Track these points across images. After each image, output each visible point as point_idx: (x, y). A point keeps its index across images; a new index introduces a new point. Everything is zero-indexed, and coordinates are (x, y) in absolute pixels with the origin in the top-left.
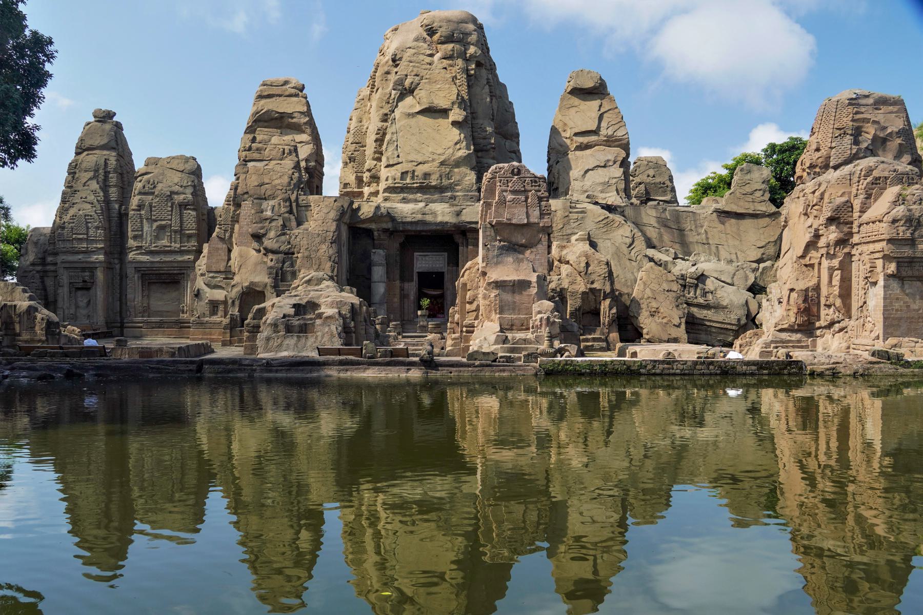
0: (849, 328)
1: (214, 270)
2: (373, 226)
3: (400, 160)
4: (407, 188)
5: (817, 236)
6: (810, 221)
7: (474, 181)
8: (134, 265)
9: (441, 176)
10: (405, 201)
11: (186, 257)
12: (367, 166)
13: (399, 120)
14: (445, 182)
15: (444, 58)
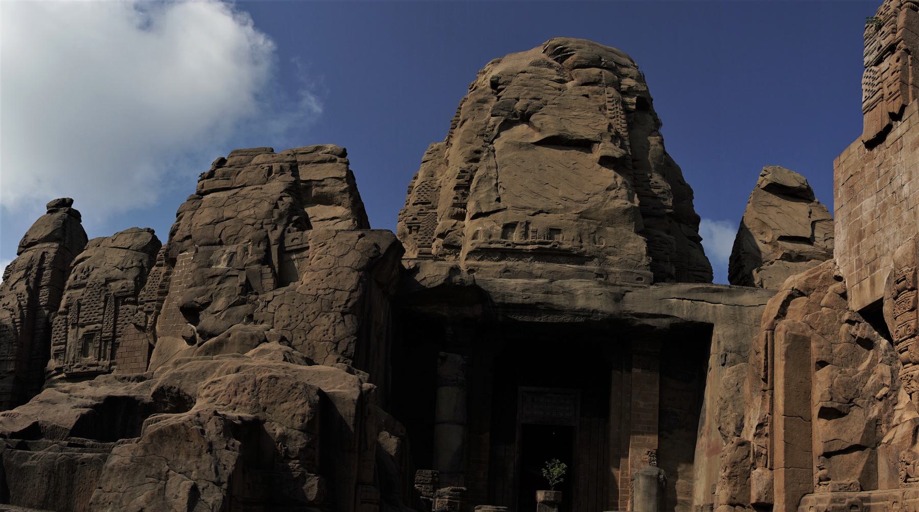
3: (501, 205)
7: (644, 250)
9: (580, 235)
12: (438, 230)
13: (501, 152)
14: (588, 247)
15: (583, 85)
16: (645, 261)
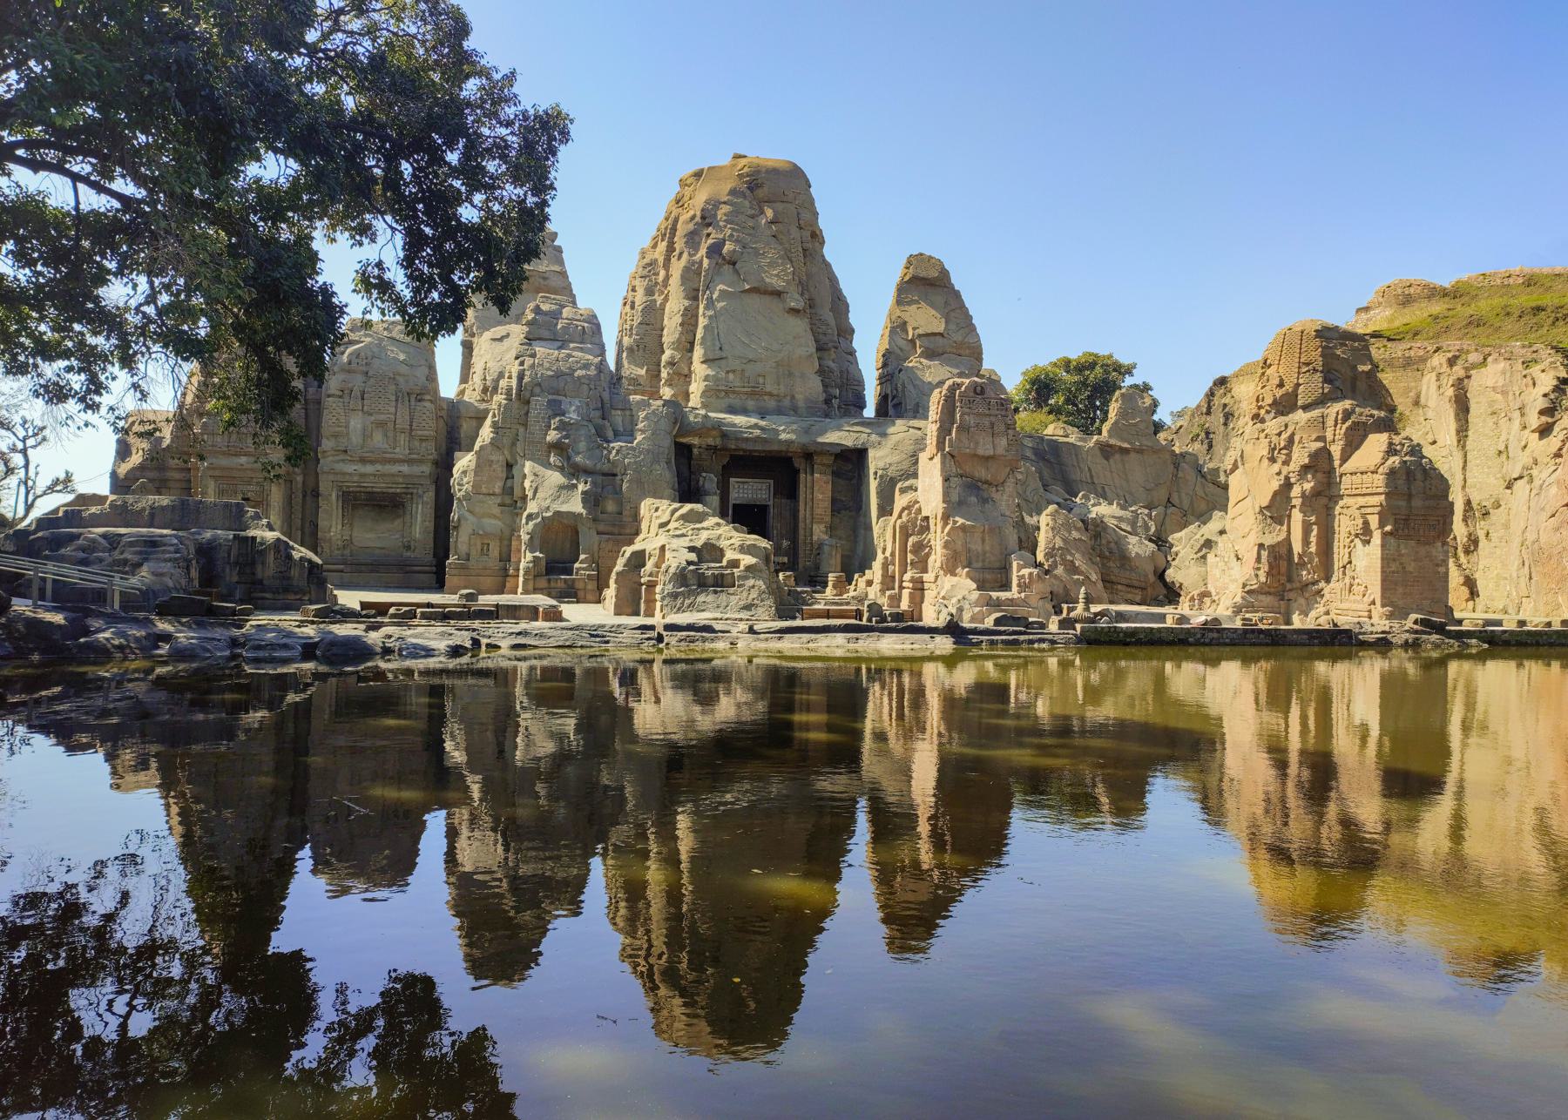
1: (484, 490)
2: (695, 441)
5: (1288, 485)
8: (331, 477)
10: (732, 410)
11: (416, 470)
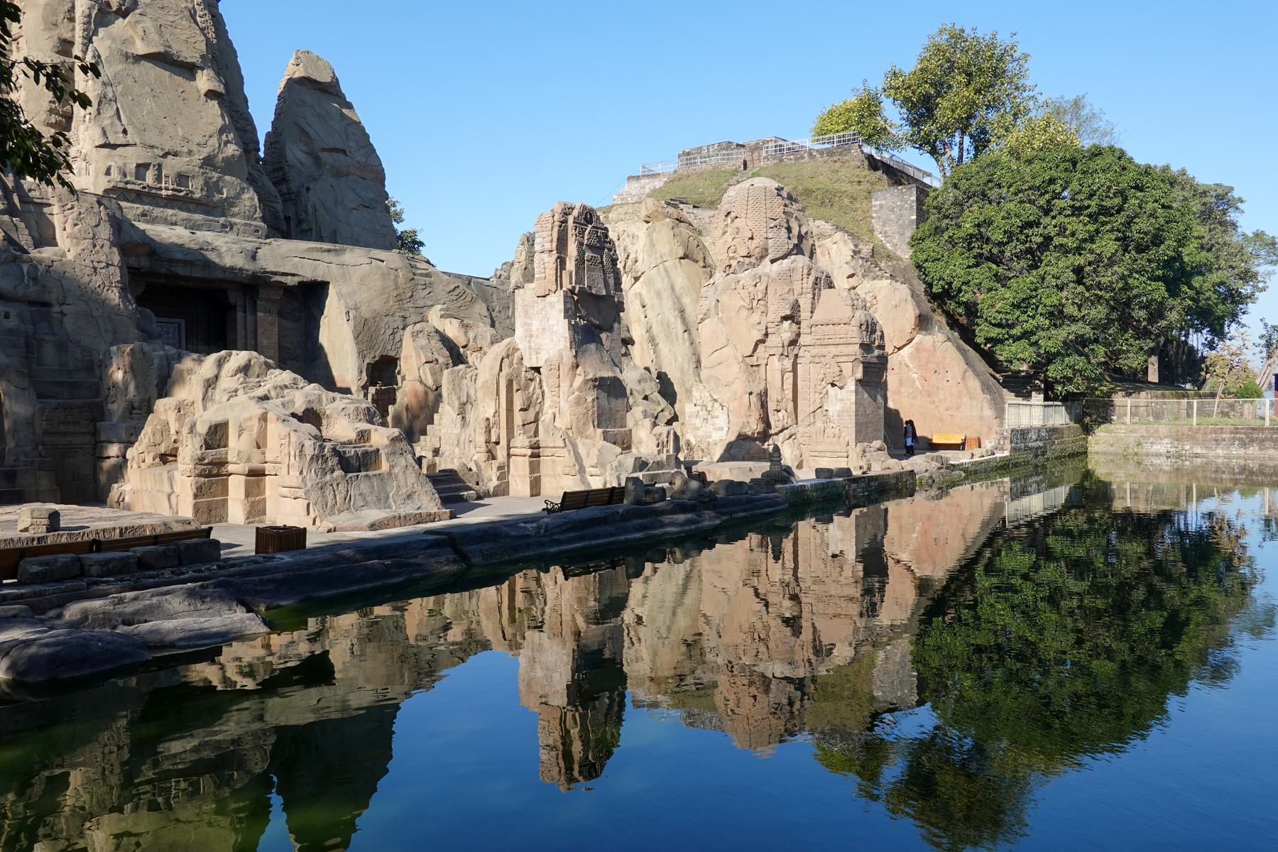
0: (798, 436)
3: (130, 138)
4: (148, 194)
6: (756, 317)
16: (259, 214)
